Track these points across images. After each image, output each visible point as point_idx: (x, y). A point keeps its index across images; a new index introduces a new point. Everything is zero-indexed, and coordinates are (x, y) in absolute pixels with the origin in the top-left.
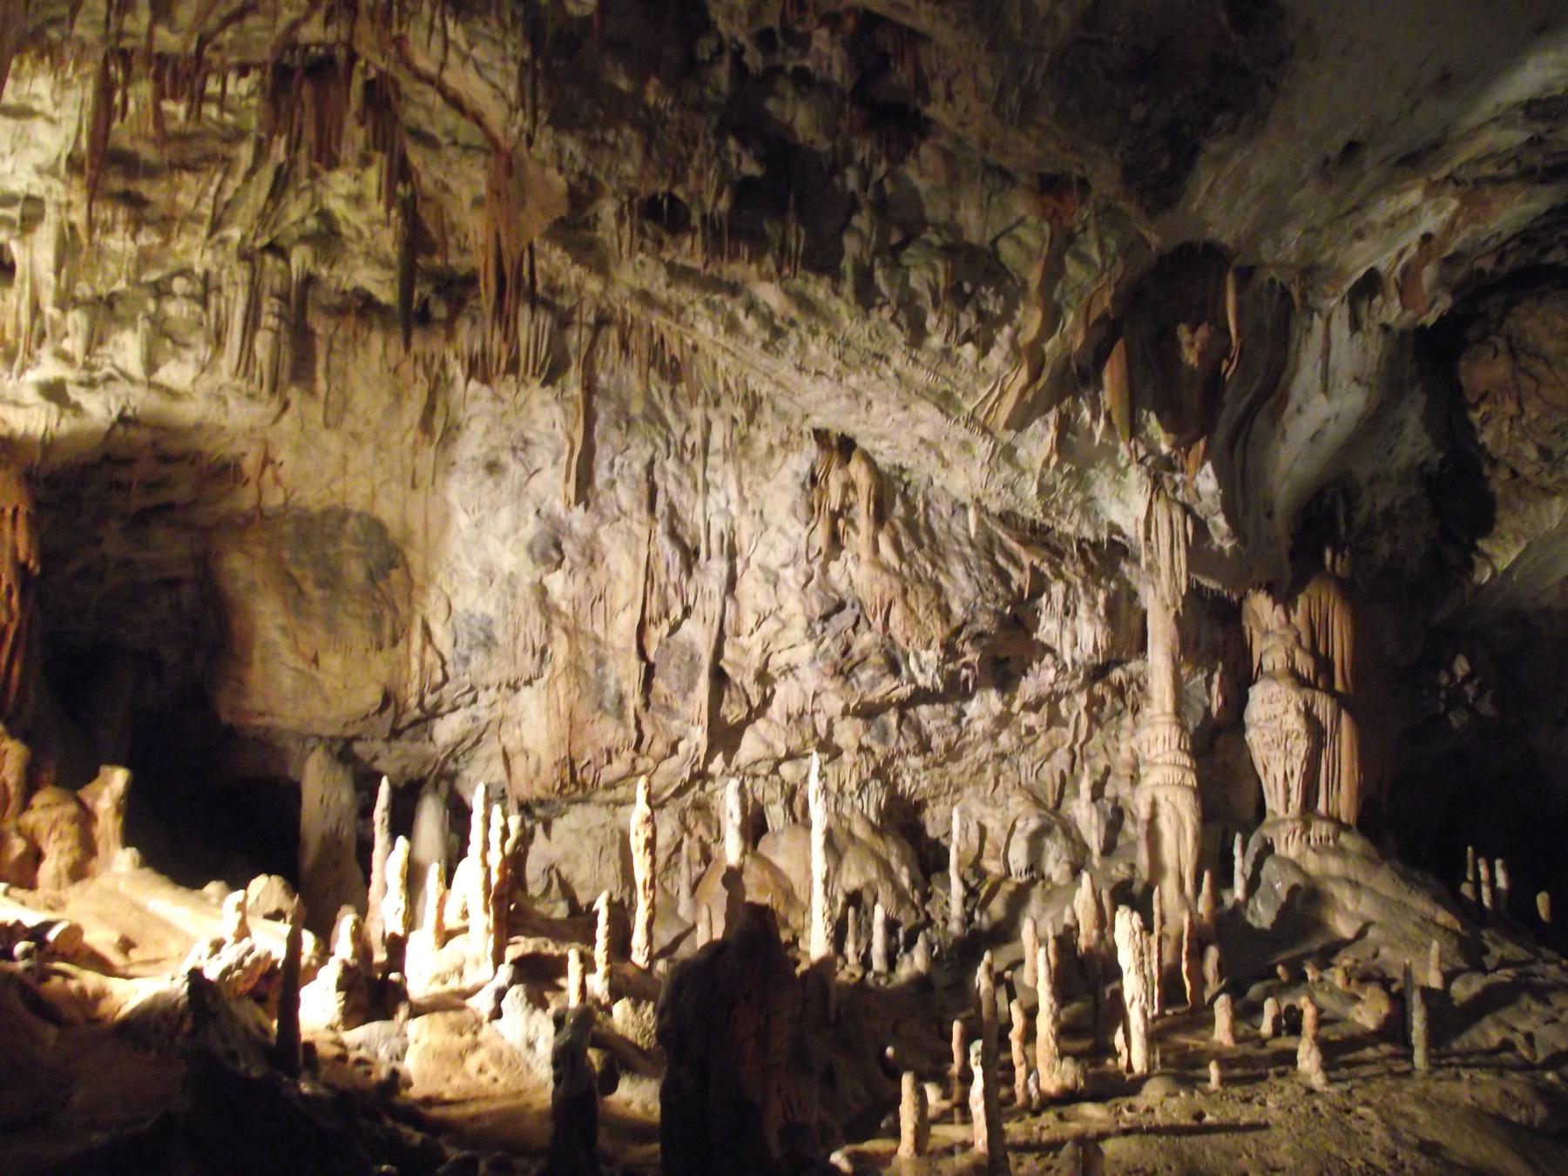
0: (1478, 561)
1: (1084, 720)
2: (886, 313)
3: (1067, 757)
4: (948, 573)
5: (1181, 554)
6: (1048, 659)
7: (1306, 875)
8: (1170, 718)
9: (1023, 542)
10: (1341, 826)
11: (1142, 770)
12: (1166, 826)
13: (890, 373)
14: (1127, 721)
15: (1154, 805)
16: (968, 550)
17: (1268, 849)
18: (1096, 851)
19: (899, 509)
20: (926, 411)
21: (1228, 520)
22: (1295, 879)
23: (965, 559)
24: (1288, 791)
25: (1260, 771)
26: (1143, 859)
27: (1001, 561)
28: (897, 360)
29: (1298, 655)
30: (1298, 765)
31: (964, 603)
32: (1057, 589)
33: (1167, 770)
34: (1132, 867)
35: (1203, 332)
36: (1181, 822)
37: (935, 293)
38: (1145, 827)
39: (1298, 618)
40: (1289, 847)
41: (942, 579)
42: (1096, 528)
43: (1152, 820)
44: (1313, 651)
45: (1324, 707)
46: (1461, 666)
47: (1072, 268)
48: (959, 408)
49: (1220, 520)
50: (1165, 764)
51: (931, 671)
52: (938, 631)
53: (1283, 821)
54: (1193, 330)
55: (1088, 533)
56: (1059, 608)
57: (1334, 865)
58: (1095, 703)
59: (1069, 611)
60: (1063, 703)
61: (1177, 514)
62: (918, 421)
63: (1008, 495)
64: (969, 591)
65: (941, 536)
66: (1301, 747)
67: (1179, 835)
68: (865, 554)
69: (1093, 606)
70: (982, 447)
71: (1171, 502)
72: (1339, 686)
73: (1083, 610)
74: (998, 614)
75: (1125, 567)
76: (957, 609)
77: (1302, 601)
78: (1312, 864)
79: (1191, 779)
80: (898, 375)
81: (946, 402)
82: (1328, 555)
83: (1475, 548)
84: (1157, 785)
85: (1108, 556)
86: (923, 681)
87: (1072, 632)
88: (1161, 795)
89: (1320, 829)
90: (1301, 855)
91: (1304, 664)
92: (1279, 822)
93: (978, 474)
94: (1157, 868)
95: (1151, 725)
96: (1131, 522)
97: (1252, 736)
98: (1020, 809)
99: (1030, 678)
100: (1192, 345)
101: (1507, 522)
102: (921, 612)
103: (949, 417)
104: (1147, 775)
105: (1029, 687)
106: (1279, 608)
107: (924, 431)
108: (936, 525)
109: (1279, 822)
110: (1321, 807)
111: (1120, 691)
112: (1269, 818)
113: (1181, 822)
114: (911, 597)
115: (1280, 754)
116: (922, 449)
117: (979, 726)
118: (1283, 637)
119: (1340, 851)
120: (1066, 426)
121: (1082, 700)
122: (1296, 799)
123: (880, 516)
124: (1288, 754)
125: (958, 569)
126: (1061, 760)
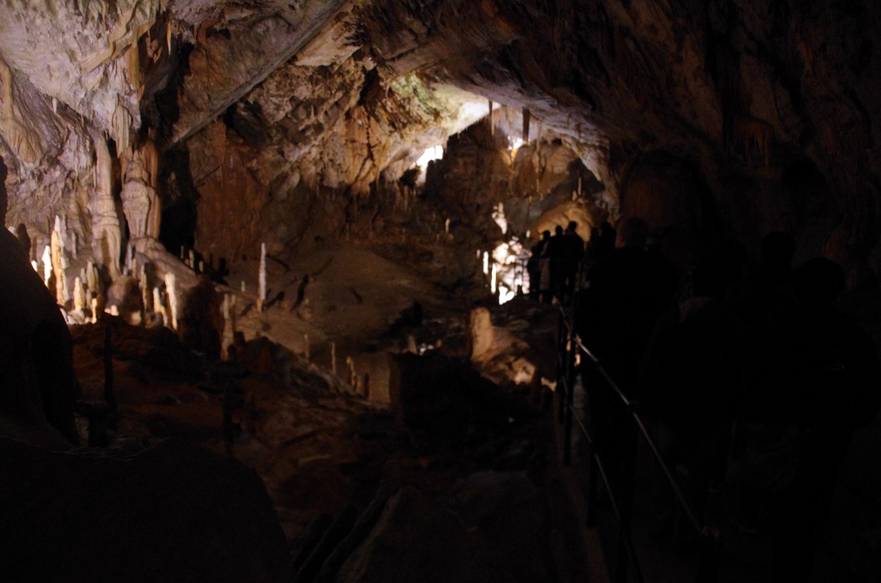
0: (174, 133)
1: (60, 193)
2: (80, 19)
3: (48, 210)
4: (38, 127)
5: (127, 131)
6: (58, 167)
7: (148, 258)
8: (109, 197)
9: (63, 116)
10: (156, 240)
11: (95, 219)
12: (110, 241)
13: (61, 40)
14: (73, 195)
15: (105, 233)
16: (44, 117)
17: (134, 249)
18: (74, 252)
19: (16, 93)
20: (64, 58)
21: (142, 118)
22: (146, 261)
23: (44, 121)
24: (140, 226)
25: (128, 218)
26: (99, 255)
27: (57, 124)
28: (67, 36)
29: (144, 172)
30: (144, 217)
31: (48, 142)
32: (74, 137)
33: (110, 219)
34: (94, 259)
35: (155, 43)
36: (115, 240)
37: (100, 15)
38: (100, 242)
39: (143, 157)
40: (141, 248)
41: (37, 130)
42: (90, 112)
43: (104, 239)
44: (147, 170)
45: (152, 193)
46: (173, 176)
47: (139, 15)
48: (76, 60)
49: (139, 118)
50: (108, 216)
51: (29, 173)
52: (39, 156)
53: (139, 238)
54: (152, 41)
55: (87, 115)
56: (74, 147)
57: (156, 255)
58: (66, 185)
59: (78, 149)
60: (53, 186)
61: (126, 113)
62: (56, 59)
63: (72, 95)
64: (49, 138)
65: (31, 108)
66: (147, 208)
67: (115, 245)
68: (9, 115)
69: (85, 146)
70: (75, 74)
71: (123, 107)
72: (153, 184)
73: (81, 149)
74: (57, 147)
75: (88, 129)
76: (44, 144)
77: (144, 148)
78: (150, 254)
79: (117, 223)
80: (64, 42)
81: (72, 56)
82: (150, 130)
83: (172, 127)
84: (105, 225)
85: (86, 125)
86: (23, 176)
87: (75, 158)
88: (108, 229)
89: (151, 241)
90: (146, 251)
91: (145, 176)
92: (137, 239)
93: (66, 85)
94: (107, 258)
95: (102, 199)
96: (105, 112)
97: (127, 205)
98: (35, 234)
99: (48, 175)
100: (151, 48)
101: (184, 118)
102: (33, 146)
103: (71, 61)
104: (100, 221)
105: (47, 179)
106: (136, 152)
107: (54, 64)
108: (27, 101)
109: (137, 239)
110: (149, 232)
111: (73, 181)
112: (132, 237)
113: (115, 240)
114: (29, 138)
115: (138, 212)
116: (46, 71)
117: (23, 196)
118: (139, 164)
119: (156, 249)
120: (106, 74)
121: (61, 186)
122: (143, 229)
123: (13, 95)
124: (141, 212)
125: (43, 126)
126: (47, 211)
